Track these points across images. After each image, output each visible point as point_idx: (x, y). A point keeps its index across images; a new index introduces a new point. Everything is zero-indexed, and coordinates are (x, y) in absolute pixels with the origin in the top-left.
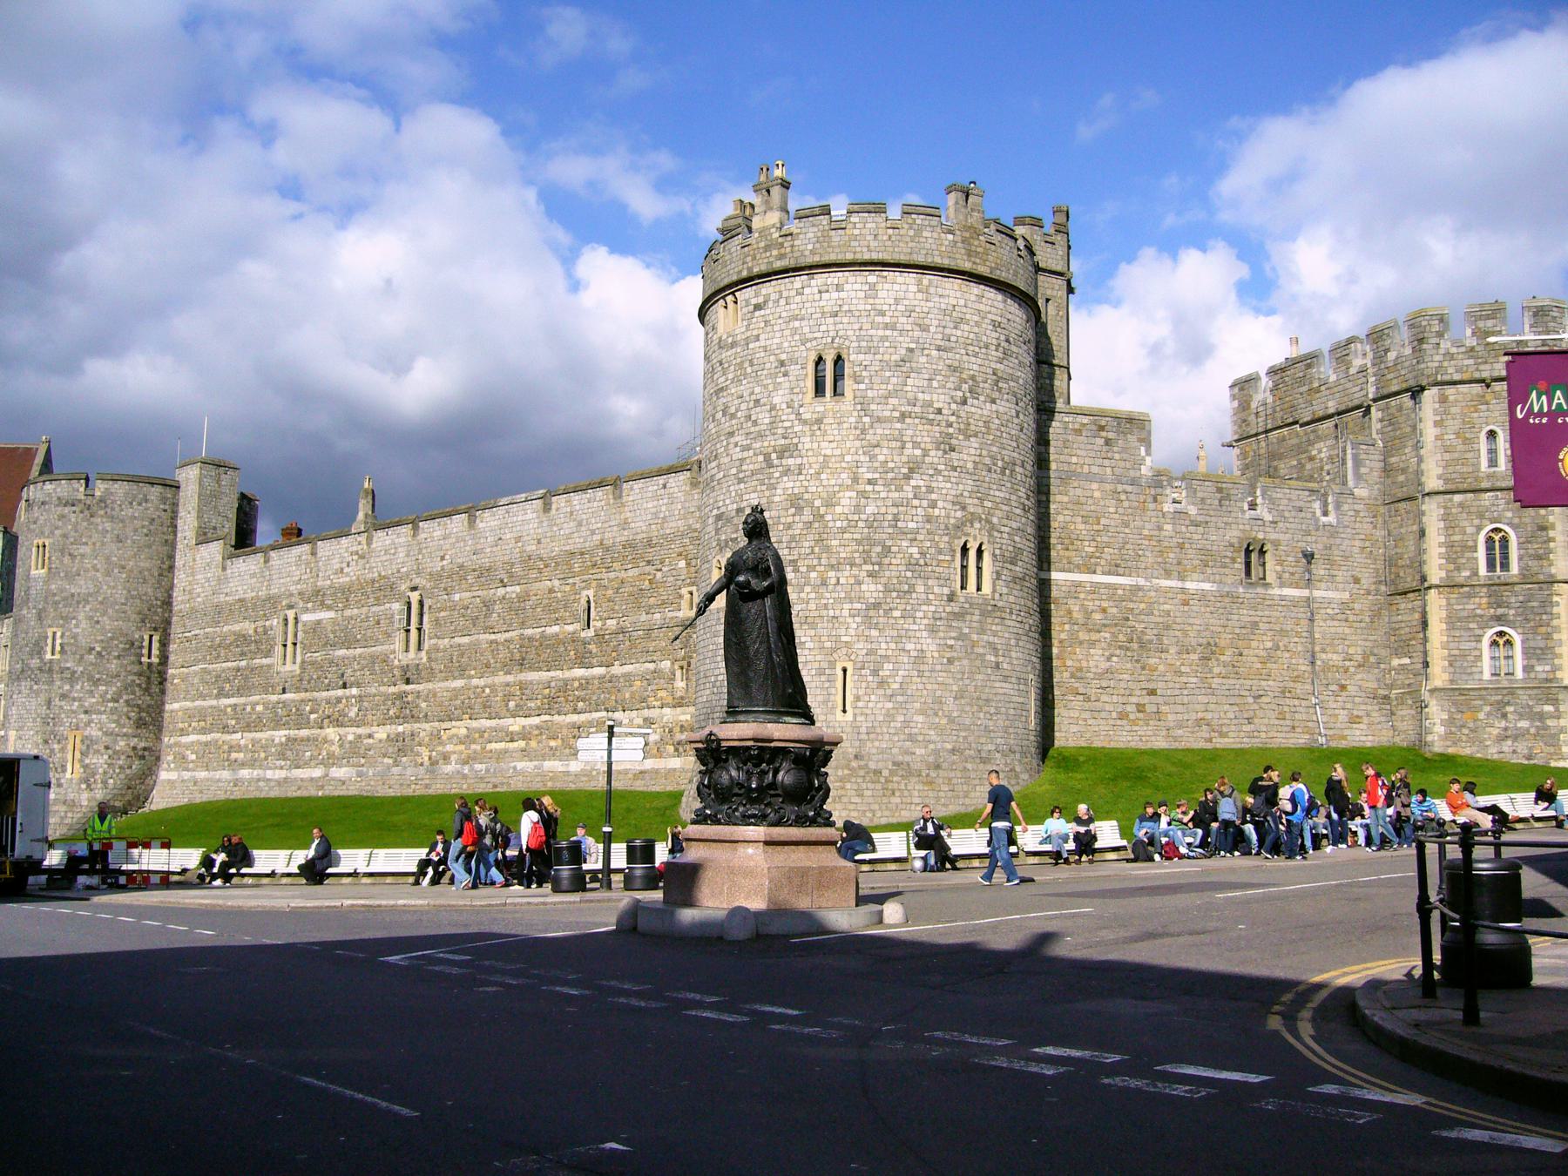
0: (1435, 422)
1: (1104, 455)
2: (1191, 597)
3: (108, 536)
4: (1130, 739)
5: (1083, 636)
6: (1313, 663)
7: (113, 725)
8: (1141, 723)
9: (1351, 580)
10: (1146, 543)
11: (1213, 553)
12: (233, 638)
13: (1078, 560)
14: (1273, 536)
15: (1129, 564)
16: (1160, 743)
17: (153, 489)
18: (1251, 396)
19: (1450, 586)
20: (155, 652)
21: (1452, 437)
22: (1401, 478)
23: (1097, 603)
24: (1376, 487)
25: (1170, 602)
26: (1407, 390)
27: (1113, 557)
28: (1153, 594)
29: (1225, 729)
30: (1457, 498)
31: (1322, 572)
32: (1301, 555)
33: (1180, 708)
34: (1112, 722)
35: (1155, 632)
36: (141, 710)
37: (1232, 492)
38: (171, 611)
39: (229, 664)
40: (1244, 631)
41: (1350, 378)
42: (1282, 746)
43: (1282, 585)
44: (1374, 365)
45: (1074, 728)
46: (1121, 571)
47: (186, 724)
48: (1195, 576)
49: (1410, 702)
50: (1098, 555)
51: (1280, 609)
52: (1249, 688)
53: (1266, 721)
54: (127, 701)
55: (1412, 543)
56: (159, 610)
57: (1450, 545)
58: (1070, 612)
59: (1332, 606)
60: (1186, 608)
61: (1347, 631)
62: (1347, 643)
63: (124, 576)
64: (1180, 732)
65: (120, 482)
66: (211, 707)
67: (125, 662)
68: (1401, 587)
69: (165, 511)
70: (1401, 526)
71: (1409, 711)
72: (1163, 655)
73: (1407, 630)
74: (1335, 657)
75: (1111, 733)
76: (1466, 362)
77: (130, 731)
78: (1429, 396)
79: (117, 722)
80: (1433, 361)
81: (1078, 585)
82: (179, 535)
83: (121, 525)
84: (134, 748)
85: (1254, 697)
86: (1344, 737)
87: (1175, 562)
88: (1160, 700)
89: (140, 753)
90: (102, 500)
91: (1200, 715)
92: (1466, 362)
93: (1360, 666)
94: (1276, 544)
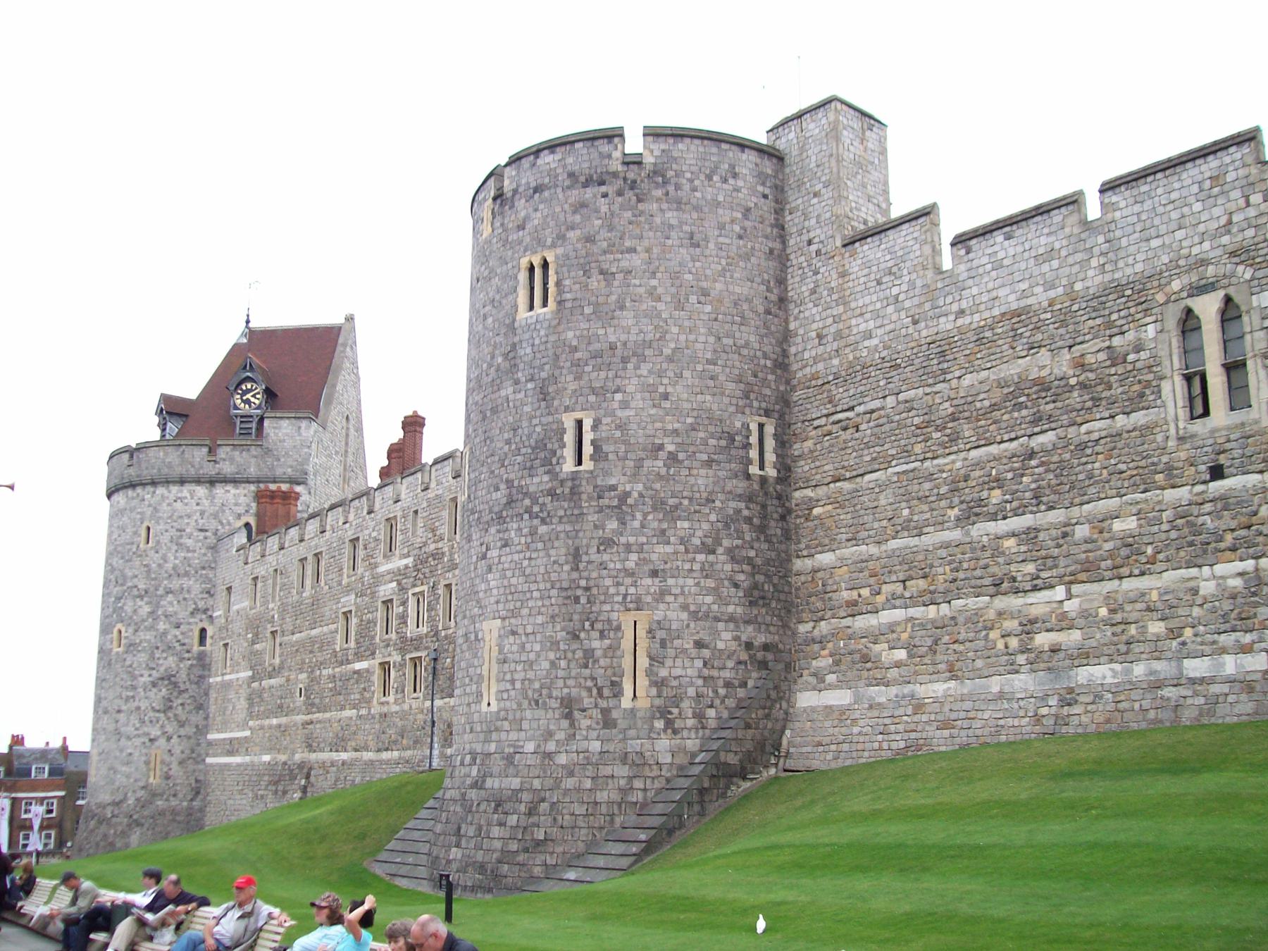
3: (673, 234)
7: (709, 599)
12: (997, 395)
17: (744, 156)
20: (770, 457)
36: (755, 569)
38: (788, 382)
39: (994, 449)
47: (865, 592)
54: (730, 551)
56: (771, 377)
63: (708, 308)
65: (688, 141)
66: (946, 545)
67: (722, 474)
69: (765, 196)
77: (739, 610)
79: (715, 591)
82: (792, 242)
83: (695, 215)
84: (749, 646)
89: (760, 655)
90: (657, 172)
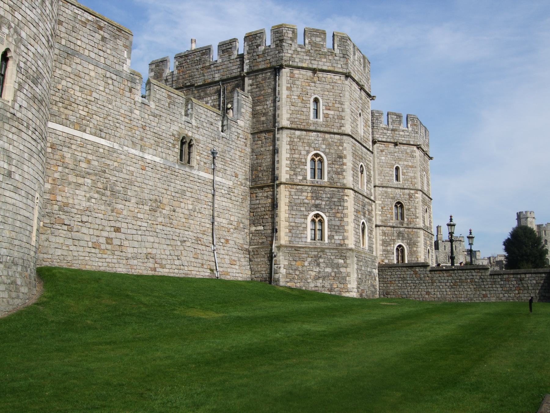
0: (287, 87)
1: (100, 47)
2: (147, 165)
4: (100, 264)
5: (72, 178)
6: (213, 223)
8: (109, 252)
9: (234, 175)
10: (123, 119)
11: (163, 138)
13: (72, 119)
14: (197, 136)
15: (110, 131)
16: (122, 269)
18: (163, 70)
19: (291, 184)
21: (296, 97)
22: (263, 119)
23: (84, 155)
24: (248, 122)
25: (134, 165)
26: (270, 68)
27: (99, 123)
28: (123, 157)
29: (164, 262)
30: (298, 133)
31: (220, 166)
32: (210, 152)
33: (136, 244)
34: (88, 250)
35: (123, 185)
37: (177, 100)
40: (177, 195)
41: (232, 61)
42: (197, 277)
43: (198, 170)
44: (248, 53)
45: (59, 252)
46: (103, 135)
48: (151, 151)
49: (263, 253)
50: (88, 118)
51: (198, 184)
52: (177, 234)
53: (188, 259)
55: (268, 157)
57: (292, 160)
58: (63, 157)
59: (224, 188)
60: (144, 172)
61: (231, 205)
62: (230, 213)
64: (135, 262)
68: (259, 184)
70: (262, 147)
71: (262, 259)
72: (127, 203)
73: (263, 209)
74: (224, 221)
75: (87, 258)
76: (305, 57)
78: (285, 71)
80: (287, 53)
81: (72, 137)
85: (181, 241)
86: (227, 273)
87: (139, 138)
88: (123, 236)
91: (149, 250)
92: (305, 57)
93: (235, 229)
94: (198, 141)
